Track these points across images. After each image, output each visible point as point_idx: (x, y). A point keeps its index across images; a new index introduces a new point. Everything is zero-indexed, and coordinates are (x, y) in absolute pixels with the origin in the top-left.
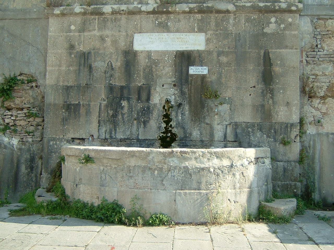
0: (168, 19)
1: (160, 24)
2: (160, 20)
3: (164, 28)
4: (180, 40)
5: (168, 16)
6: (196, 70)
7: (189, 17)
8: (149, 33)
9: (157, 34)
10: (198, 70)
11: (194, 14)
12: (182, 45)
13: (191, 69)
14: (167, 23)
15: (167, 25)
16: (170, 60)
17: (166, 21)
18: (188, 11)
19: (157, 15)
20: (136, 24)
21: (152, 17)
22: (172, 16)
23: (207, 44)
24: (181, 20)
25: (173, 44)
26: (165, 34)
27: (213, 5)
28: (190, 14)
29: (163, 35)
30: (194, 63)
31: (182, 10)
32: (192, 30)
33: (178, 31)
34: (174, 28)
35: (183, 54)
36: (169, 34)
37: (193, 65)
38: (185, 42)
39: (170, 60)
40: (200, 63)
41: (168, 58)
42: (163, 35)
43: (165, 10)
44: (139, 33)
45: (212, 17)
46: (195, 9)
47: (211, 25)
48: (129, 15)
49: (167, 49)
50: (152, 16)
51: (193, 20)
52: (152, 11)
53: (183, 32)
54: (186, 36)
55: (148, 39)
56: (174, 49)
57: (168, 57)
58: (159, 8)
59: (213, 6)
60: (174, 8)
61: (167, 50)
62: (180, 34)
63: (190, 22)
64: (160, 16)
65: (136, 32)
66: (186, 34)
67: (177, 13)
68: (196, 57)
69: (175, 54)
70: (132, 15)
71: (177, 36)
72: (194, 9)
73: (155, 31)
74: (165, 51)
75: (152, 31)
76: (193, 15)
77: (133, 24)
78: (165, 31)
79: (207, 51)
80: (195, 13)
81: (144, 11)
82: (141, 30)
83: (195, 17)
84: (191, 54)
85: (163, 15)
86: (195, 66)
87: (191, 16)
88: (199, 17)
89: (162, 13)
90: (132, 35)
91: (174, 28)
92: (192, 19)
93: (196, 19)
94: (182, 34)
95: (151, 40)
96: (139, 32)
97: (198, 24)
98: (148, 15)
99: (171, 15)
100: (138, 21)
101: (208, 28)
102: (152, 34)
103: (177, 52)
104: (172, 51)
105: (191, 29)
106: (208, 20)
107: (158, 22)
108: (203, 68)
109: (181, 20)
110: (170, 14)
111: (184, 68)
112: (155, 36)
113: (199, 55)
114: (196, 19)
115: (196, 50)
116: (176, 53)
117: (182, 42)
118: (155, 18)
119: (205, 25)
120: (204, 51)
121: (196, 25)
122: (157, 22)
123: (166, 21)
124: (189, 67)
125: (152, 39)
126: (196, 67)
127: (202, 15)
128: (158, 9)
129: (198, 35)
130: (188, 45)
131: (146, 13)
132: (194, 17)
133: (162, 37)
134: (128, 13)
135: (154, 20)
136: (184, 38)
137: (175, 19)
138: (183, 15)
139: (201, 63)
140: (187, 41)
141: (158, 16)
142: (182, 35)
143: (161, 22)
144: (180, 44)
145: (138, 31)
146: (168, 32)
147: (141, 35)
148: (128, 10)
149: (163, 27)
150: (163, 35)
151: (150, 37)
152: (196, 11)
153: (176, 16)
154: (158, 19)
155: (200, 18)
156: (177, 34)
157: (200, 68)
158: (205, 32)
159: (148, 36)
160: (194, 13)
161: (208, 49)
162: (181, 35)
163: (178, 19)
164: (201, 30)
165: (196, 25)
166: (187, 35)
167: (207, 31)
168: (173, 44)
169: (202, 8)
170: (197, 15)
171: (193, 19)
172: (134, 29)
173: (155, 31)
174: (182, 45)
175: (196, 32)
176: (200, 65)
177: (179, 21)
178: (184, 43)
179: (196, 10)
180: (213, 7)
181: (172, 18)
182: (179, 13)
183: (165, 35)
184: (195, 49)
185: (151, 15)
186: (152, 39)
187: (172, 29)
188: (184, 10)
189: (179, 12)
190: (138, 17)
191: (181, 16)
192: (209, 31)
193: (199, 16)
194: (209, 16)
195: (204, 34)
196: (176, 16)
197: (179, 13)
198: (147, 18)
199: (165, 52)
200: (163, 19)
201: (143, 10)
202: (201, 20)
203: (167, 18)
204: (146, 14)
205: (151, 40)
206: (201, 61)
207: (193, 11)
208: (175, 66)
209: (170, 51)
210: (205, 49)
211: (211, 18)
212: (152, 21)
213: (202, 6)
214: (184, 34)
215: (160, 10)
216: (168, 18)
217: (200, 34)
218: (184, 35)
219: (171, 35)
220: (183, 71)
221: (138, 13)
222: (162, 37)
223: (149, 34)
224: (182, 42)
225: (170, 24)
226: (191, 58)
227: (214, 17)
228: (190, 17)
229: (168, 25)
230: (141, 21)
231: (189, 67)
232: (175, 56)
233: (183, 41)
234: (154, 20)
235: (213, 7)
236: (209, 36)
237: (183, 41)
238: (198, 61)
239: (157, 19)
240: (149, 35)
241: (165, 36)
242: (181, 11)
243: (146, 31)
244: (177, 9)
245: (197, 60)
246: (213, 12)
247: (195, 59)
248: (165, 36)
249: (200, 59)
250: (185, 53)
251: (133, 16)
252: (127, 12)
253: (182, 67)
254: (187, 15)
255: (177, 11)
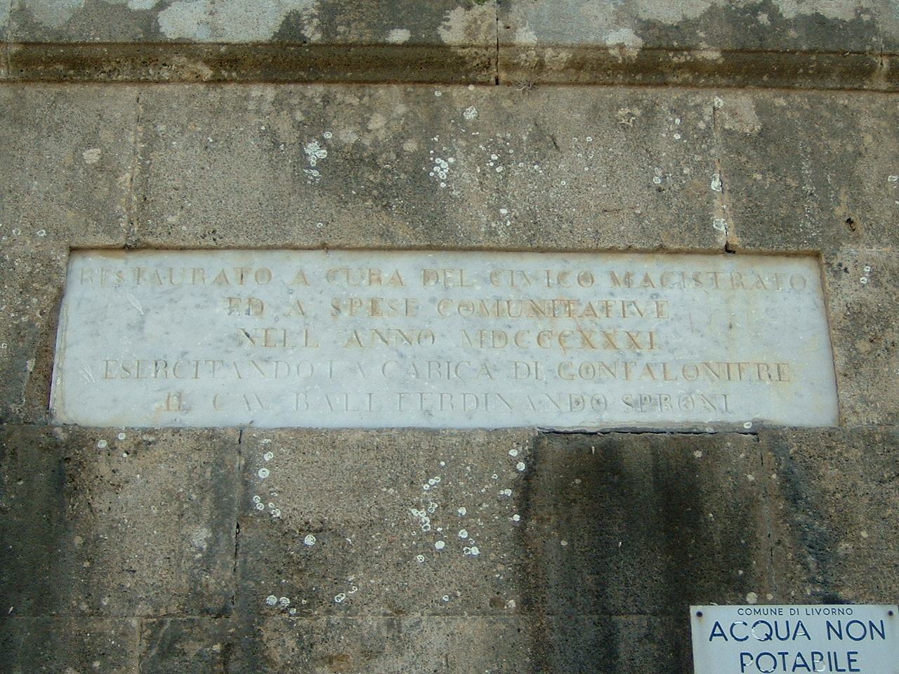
0: (432, 125)
1: (347, 169)
2: (349, 136)
3: (394, 206)
4: (565, 324)
5: (430, 101)
6: (775, 646)
7: (637, 112)
8: (228, 248)
9: (315, 263)
10: (793, 647)
11: (685, 84)
12: (585, 371)
13: (717, 632)
14: (422, 160)
15: (421, 179)
16: (463, 534)
17: (410, 146)
18: (634, 54)
19: (316, 91)
20: (100, 167)
21: (266, 107)
22: (470, 104)
23: (850, 369)
24: (559, 141)
25: (488, 369)
26: (404, 265)
27: (867, 11)
28: (650, 91)
29: (375, 278)
30: (745, 565)
31: (569, 42)
32: (679, 236)
33: (533, 240)
34: (494, 209)
35: (616, 470)
36: (442, 262)
37: (732, 589)
38: (620, 345)
39: (463, 534)
40: (805, 566)
41: (445, 514)
42: (375, 278)
43: (399, 36)
44: (127, 248)
45: (865, 122)
46: (702, 35)
47: (869, 187)
48: (26, 81)
49: (429, 413)
50: (270, 92)
51: (685, 136)
52: (270, 44)
53: (590, 243)
54: (618, 289)
55: (221, 309)
56: (504, 418)
57: (447, 496)
58: (338, 18)
59: (866, 18)
60: (490, 26)
61: (423, 423)
62: (554, 264)
63: (654, 159)
64: (347, 96)
65: (91, 241)
66: (620, 265)
67: (520, 76)
68: (752, 502)
69: (521, 466)
70: (61, 80)
71: (536, 290)
72: (693, 34)
73: (296, 231)
74: (403, 431)
75: (269, 237)
76: (675, 94)
77: (69, 161)
78: (403, 233)
79: (868, 438)
80: (700, 74)
81: (184, 46)
82: (143, 225)
83: (701, 117)
84: (692, 466)
85: (382, 91)
86: (751, 597)
87: (664, 108)
88: (734, 114)
89: (368, 65)
90: (49, 263)
91: (494, 209)
92: (670, 131)
93: (706, 135)
94: (577, 265)
95: (252, 324)
96: (121, 240)
97: (736, 173)
98: (229, 88)
99: (456, 92)
100: (120, 132)
101: (839, 211)
102: (258, 261)
103: (541, 443)
104: (481, 439)
105: (668, 219)
106: (835, 144)
107: (323, 154)
108: (845, 620)
109: (559, 132)
110: (446, 83)
111: (631, 627)
112: (297, 282)
113: (786, 477)
114: (706, 135)
115: (747, 426)
116: (534, 458)
117: (586, 342)
118: (299, 116)
119: (808, 188)
120: (830, 433)
121: (715, 184)
122: (315, 152)
123: (410, 146)
124: (694, 610)
125: (258, 307)
126: (769, 613)
127: (766, 95)
128: (327, 28)
129: (749, 280)
130: (658, 374)
131: (207, 62)
132: (692, 114)
133: (374, 290)
134: (19, 54)
135: (284, 126)
136: (606, 308)
137: (503, 125)
138: (579, 90)
139: (821, 560)
140: (643, 339)
141: (326, 100)
142: (586, 278)
143: (358, 146)
144: (563, 366)
145: (111, 229)
146: (430, 248)
147: (139, 273)
148: (22, 35)
149: (383, 197)
150: (385, 276)
151: (235, 288)
152: (713, 55)
153: (506, 104)
154: (326, 125)
155: (750, 122)
156: (532, 264)
157: (815, 617)
158: (817, 255)
159: (222, 279)
160: (688, 76)
161: (875, 418)
162: (572, 280)
163: (531, 128)
164: (770, 234)
165: (715, 184)
166: (638, 280)
167: (836, 242)
168: (488, 369)
169: (763, 28)
170: (719, 102)
171: (679, 131)
172: (70, 214)
173: (296, 231)
174: (585, 371)
175: (729, 250)
176: (812, 581)
177: (545, 142)
178: (608, 356)
179: (711, 41)
180: (871, 26)
181: (470, 114)
182: (538, 75)
183: (402, 275)
184: (732, 418)
185: (256, 91)
186: (258, 307)
187: (474, 216)
188: (591, 39)
189: (541, 65)
190: (120, 100)
191: (564, 105)
192: (856, 240)
193: (737, 108)
194: (832, 108)
195: (802, 270)
196: (506, 104)
197: (538, 75)
198: (217, 112)
199: (401, 441)
200: (377, 122)
201: (174, 37)
202: (763, 138)
203: (423, 118)
204: (207, 73)
205: (252, 324)
206: (821, 548)
207: (677, 51)
208: (527, 604)
209: (466, 436)
210: (841, 421)
211: (852, 125)
212: (266, 143)
213: (763, 18)
214: (602, 267)
215: (353, 38)
216: (435, 118)
217: (767, 270)
218: (603, 282)
219: (470, 276)
220: (623, 656)
221: (127, 67)
222: (374, 290)
223: (227, 262)
224: (586, 342)
225: (452, 167)
226: (698, 511)
227: (882, 116)
228: (650, 112)
229: (436, 183)
230: (151, 141)
231: (694, 610)
232: (526, 489)
233: (598, 339)
234: (284, 126)
235: (871, 26)
236: (856, 289)
237: (598, 339)
238: (787, 541)
239: (314, 125)
240: (232, 276)
241: (397, 280)
242: (564, 55)
243: (199, 229)
244: (525, 37)
245: (768, 520)
246: (873, 67)
247: (743, 517)
248: (397, 280)
249: (800, 518)
250: (636, 458)
251: (69, 89)
252: (14, 49)
253: (605, 612)
254: (622, 93)
255: (527, 48)
